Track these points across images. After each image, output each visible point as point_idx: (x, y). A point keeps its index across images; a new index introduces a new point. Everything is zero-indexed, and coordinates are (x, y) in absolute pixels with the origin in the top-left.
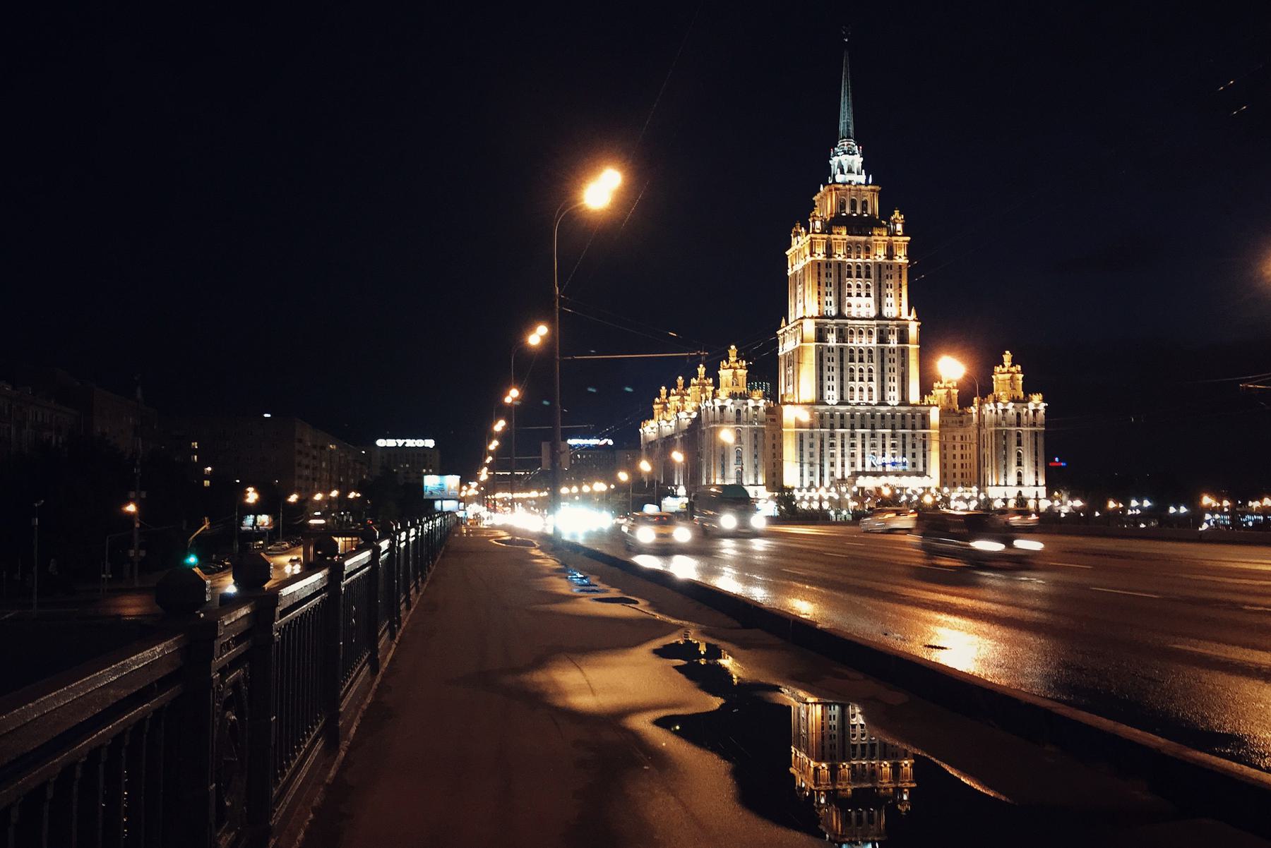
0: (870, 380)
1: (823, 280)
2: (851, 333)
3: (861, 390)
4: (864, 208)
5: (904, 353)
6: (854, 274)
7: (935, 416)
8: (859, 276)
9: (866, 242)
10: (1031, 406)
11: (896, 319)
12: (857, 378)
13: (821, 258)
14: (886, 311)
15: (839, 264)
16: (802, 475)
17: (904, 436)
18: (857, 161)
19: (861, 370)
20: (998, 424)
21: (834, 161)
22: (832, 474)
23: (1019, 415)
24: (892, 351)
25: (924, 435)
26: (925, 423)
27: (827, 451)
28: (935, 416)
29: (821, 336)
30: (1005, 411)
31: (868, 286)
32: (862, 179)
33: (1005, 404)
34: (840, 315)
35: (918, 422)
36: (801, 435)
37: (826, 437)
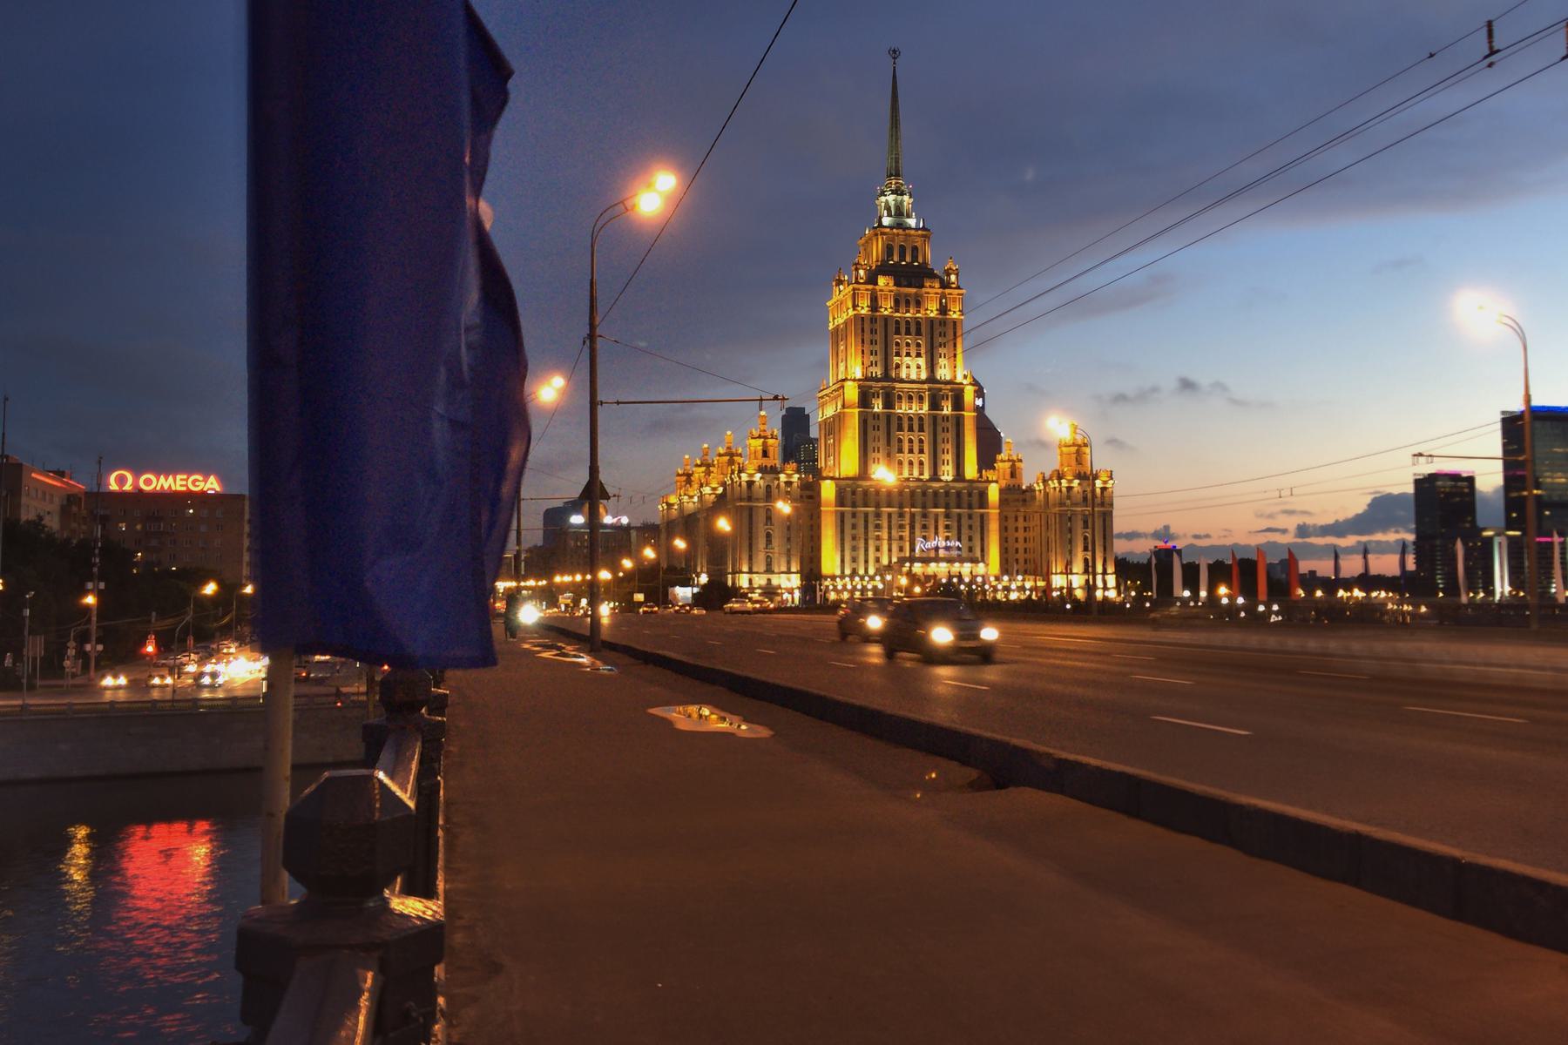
0: (921, 451)
1: (867, 337)
2: (900, 397)
3: (911, 463)
4: (915, 258)
5: (959, 422)
7: (993, 493)
8: (908, 333)
13: (864, 311)
14: (943, 373)
15: (886, 319)
16: (843, 561)
17: (959, 515)
19: (911, 441)
20: (1062, 504)
22: (877, 560)
24: (945, 418)
25: (982, 516)
27: (872, 533)
28: (993, 493)
29: (865, 400)
30: (1069, 489)
31: (918, 345)
33: (1070, 481)
34: (886, 376)
35: (975, 499)
36: (842, 514)
37: (871, 518)
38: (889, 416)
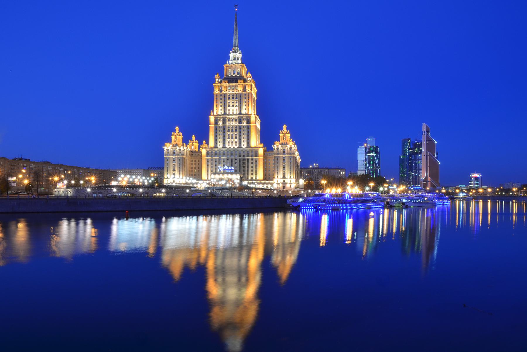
0: (236, 138)
1: (219, 101)
2: (229, 120)
3: (232, 142)
5: (248, 128)
6: (231, 98)
8: (233, 98)
9: (236, 86)
10: (289, 146)
11: (247, 114)
12: (230, 137)
14: (243, 112)
15: (225, 95)
18: (239, 55)
21: (231, 55)
23: (284, 149)
25: (256, 159)
26: (256, 154)
29: (216, 122)
30: (278, 148)
32: (240, 62)
36: (208, 159)
38: (224, 128)
